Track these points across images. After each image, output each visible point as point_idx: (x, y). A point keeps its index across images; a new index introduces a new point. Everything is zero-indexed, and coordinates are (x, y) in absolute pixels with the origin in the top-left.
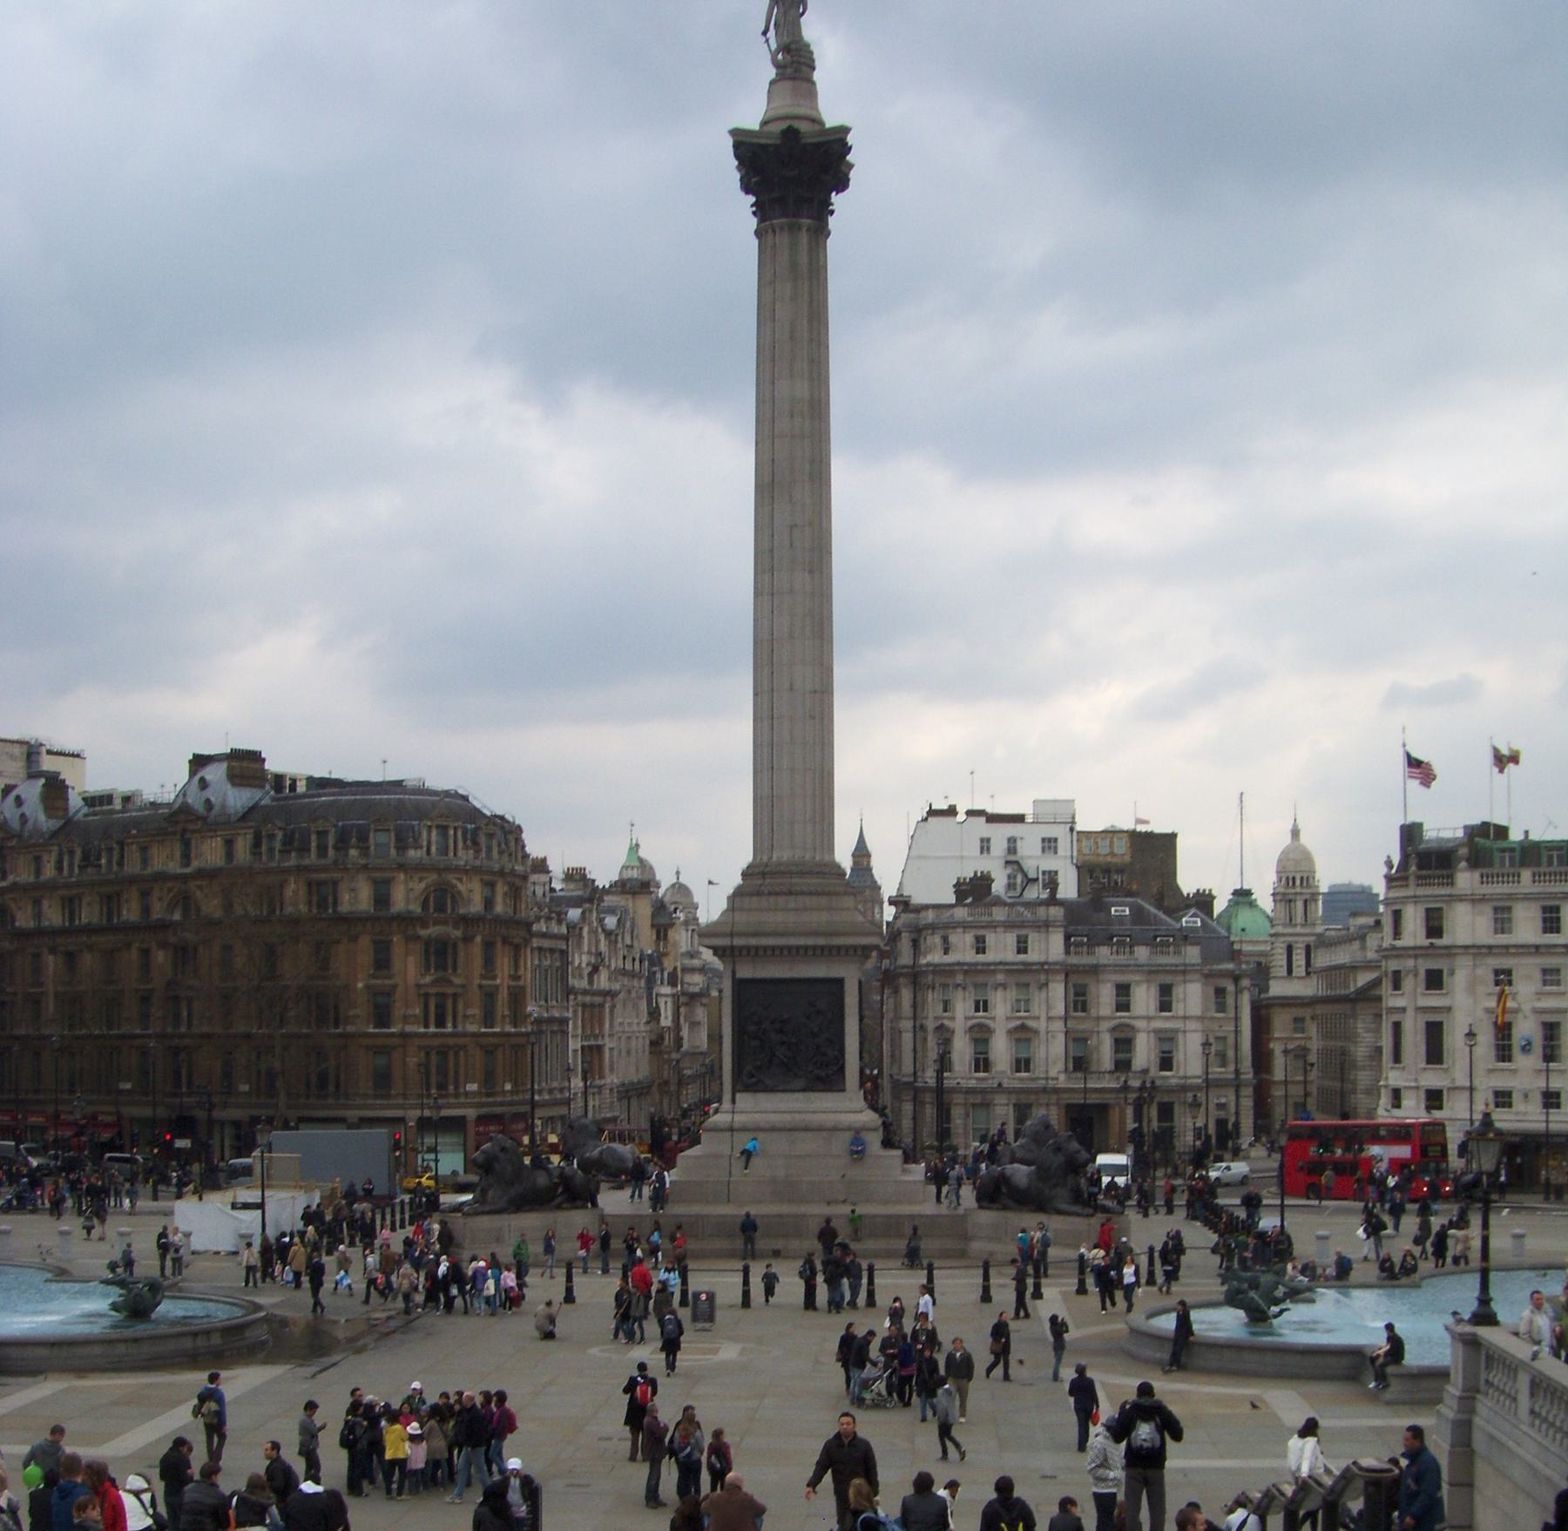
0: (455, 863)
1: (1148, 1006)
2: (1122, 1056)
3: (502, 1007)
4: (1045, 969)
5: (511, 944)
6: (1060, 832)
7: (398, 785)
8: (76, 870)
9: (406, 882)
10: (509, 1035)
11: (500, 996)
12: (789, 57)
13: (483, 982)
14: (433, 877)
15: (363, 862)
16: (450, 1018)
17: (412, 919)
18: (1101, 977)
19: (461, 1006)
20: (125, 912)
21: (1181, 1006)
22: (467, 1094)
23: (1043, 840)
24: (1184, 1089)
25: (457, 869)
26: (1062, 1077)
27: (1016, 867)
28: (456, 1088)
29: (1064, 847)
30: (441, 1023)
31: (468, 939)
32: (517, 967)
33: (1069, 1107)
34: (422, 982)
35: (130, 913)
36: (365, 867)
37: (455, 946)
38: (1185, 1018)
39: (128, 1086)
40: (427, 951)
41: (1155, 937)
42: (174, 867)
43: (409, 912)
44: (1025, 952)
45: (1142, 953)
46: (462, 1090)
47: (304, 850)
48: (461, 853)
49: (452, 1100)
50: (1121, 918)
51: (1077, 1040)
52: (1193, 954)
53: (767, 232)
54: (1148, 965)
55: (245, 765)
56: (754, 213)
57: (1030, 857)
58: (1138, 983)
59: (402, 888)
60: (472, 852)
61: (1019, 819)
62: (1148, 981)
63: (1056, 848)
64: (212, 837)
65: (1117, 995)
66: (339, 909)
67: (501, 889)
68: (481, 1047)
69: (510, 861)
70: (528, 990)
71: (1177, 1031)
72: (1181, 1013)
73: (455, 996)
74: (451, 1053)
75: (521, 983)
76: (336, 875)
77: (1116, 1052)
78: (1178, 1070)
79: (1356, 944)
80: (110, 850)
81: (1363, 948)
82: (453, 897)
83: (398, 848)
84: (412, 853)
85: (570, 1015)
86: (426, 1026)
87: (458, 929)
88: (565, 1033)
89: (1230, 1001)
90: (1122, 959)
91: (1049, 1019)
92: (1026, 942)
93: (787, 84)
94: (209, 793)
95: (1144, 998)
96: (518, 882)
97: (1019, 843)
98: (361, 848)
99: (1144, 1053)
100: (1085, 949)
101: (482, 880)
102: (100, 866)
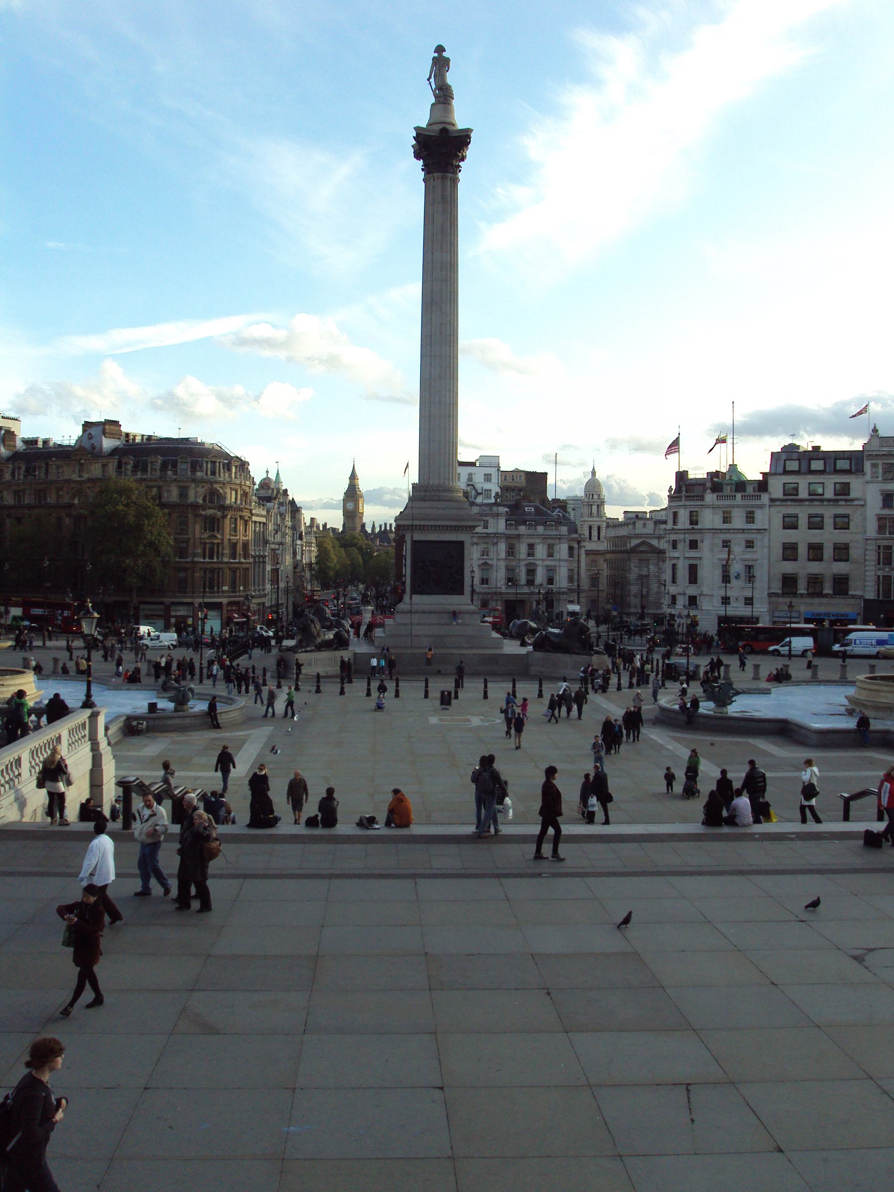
1: (543, 555)
2: (530, 578)
4: (496, 537)
6: (493, 471)
7: (187, 439)
8: (22, 477)
9: (195, 488)
10: (242, 563)
12: (442, 93)
14: (208, 486)
15: (175, 477)
16: (215, 555)
17: (198, 506)
18: (521, 540)
19: (220, 549)
20: (48, 499)
21: (558, 554)
22: (223, 592)
23: (485, 475)
24: (559, 593)
25: (219, 482)
26: (504, 587)
27: (472, 487)
28: (218, 588)
29: (494, 479)
30: (211, 557)
31: (224, 517)
33: (507, 601)
34: (202, 537)
35: (51, 499)
36: (175, 480)
37: (218, 520)
38: (560, 560)
39: (49, 585)
40: (205, 523)
41: (546, 522)
42: (75, 477)
43: (196, 502)
44: (487, 528)
45: (540, 529)
46: (220, 590)
47: (145, 470)
48: (222, 475)
49: (216, 595)
50: (530, 513)
51: (510, 570)
52: (564, 530)
53: (430, 179)
54: (543, 535)
55: (110, 427)
56: (423, 170)
57: (478, 483)
58: (539, 544)
59: (193, 490)
61: (472, 464)
62: (543, 543)
63: (491, 478)
64: (96, 463)
65: (528, 549)
66: (162, 500)
68: (230, 569)
71: (555, 566)
72: (558, 558)
73: (218, 544)
74: (216, 571)
76: (161, 484)
77: (528, 575)
78: (556, 584)
79: (631, 527)
80: (40, 467)
81: (634, 528)
82: (218, 495)
83: (191, 472)
84: (199, 474)
85: (267, 554)
86: (204, 558)
87: (219, 511)
88: (264, 562)
89: (576, 552)
90: (531, 532)
91: (498, 559)
92: (487, 523)
93: (442, 106)
94: (93, 441)
95: (541, 551)
96: (247, 490)
97: (474, 476)
98: (173, 471)
99: (540, 577)
100: (514, 527)
102: (35, 475)
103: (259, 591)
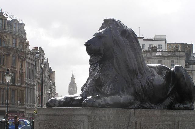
3: (18, 78)
5: (21, 58)
13: (12, 69)
31: (8, 55)
32: (22, 67)
48: (6, 27)
70: (25, 73)
75: (23, 71)
101: (13, 37)
103: (30, 106)
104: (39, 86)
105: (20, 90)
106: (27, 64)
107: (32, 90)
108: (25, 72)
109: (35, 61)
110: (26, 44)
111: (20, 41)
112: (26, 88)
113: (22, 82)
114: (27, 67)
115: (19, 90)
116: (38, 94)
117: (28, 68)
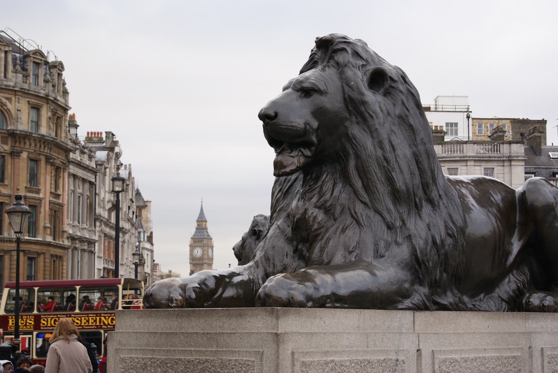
0: (5, 83)
11: (42, 210)
31: (15, 154)
32: (57, 188)
48: (10, 74)
60: (21, 75)
67: (45, 113)
69: (54, 91)
70: (65, 208)
75: (60, 201)
87: (7, 144)
101: (28, 102)
104: (106, 244)
105: (52, 255)
106: (71, 179)
107: (86, 255)
108: (66, 202)
109: (94, 172)
110: (67, 124)
111: (50, 114)
112: (70, 250)
113: (56, 231)
114: (72, 188)
115: (48, 256)
116: (104, 268)
117: (73, 191)
